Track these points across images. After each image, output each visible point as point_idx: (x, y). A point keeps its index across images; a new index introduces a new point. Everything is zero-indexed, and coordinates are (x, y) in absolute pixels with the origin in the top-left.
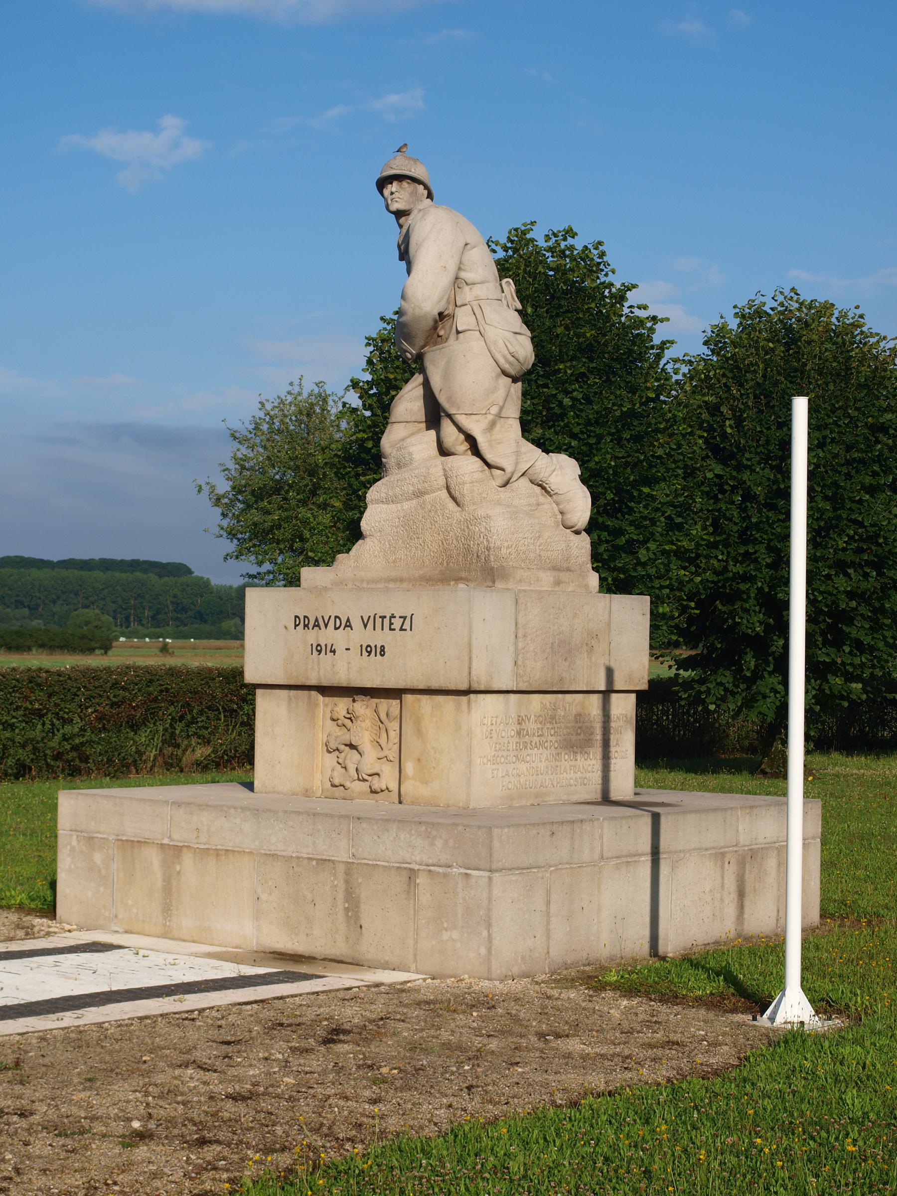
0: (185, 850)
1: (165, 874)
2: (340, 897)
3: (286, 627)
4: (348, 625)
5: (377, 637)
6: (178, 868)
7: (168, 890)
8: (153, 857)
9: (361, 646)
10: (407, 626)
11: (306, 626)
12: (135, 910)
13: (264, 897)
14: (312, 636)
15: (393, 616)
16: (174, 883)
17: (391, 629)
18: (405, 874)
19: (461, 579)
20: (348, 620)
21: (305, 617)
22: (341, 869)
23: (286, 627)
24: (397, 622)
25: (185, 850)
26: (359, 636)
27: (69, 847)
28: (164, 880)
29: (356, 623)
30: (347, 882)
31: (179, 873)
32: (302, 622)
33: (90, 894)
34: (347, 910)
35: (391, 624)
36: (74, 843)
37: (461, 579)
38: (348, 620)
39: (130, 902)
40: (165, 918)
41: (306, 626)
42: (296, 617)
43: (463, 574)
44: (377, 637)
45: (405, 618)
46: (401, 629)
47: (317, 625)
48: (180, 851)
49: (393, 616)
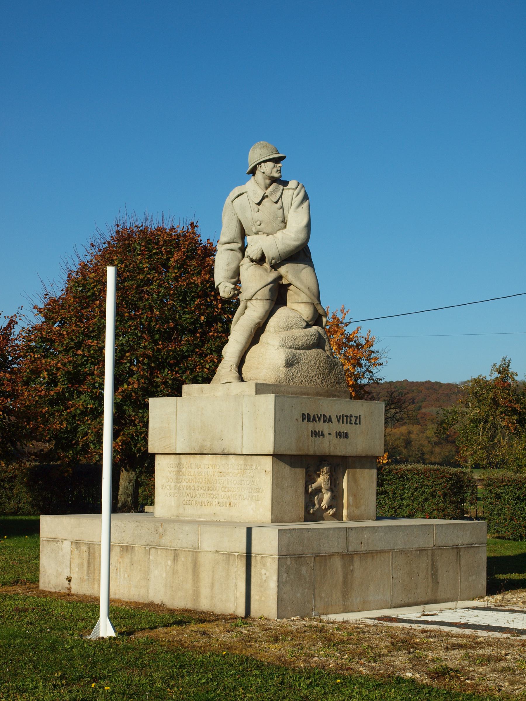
0: (355, 556)
1: (344, 573)
2: (430, 568)
3: (297, 420)
4: (330, 420)
5: (344, 428)
6: (351, 568)
7: (345, 583)
8: (337, 563)
9: (336, 432)
10: (358, 422)
11: (309, 420)
12: (326, 600)
13: (395, 576)
14: (311, 426)
15: (351, 416)
16: (349, 577)
17: (351, 423)
18: (455, 550)
19: (336, 395)
20: (330, 417)
21: (308, 414)
22: (430, 553)
23: (297, 420)
24: (353, 419)
25: (355, 556)
26: (336, 427)
27: (285, 567)
28: (344, 577)
29: (334, 419)
30: (432, 560)
31: (352, 571)
32: (306, 418)
33: (299, 595)
34: (432, 575)
35: (351, 420)
36: (289, 563)
37: (336, 395)
38: (330, 417)
39: (323, 595)
40: (344, 601)
41: (309, 420)
42: (303, 414)
43: (337, 393)
44: (344, 428)
45: (356, 417)
46: (356, 423)
47: (314, 419)
48: (353, 557)
49: (351, 416)
